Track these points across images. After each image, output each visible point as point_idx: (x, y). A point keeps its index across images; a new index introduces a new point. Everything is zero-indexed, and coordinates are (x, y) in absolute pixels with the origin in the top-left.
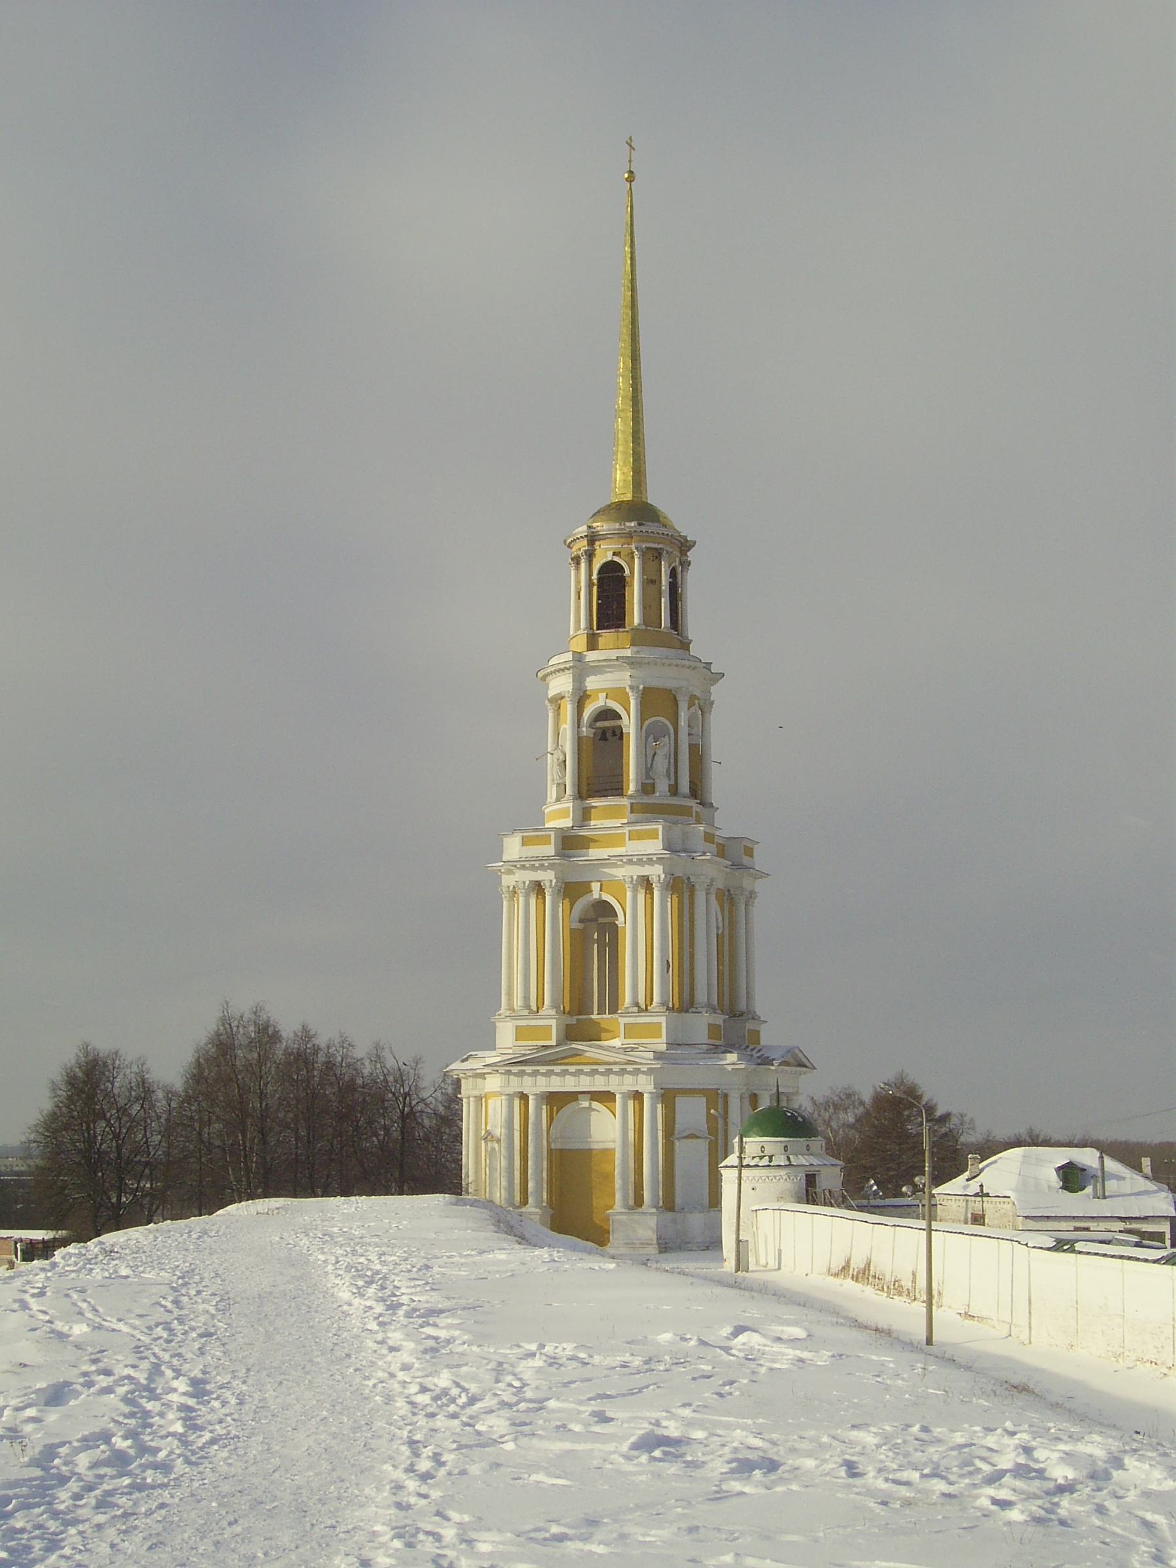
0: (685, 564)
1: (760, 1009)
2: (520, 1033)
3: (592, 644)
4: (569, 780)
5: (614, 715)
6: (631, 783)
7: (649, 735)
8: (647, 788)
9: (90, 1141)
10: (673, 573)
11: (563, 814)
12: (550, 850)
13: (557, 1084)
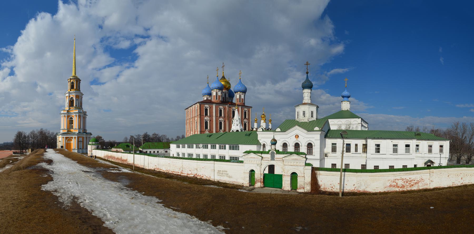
0: (80, 82)
1: (87, 129)
2: (63, 131)
3: (70, 91)
4: (68, 105)
5: (73, 98)
6: (75, 105)
7: (76, 100)
8: (76, 106)
9: (20, 141)
10: (79, 83)
12: (66, 112)
13: (67, 136)
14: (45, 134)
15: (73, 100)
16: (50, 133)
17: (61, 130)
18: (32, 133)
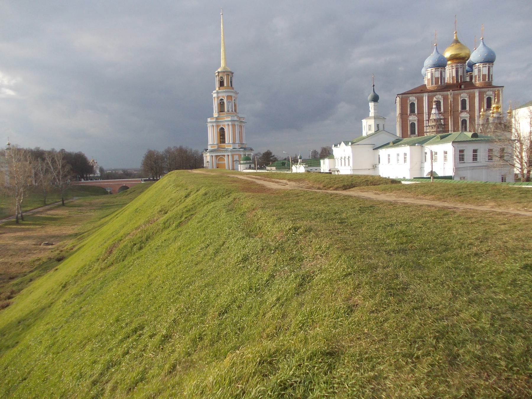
0: (233, 76)
2: (211, 147)
3: (219, 89)
5: (223, 100)
7: (228, 102)
8: (228, 111)
10: (231, 78)
11: (216, 115)
13: (217, 154)
14: (186, 152)
15: (224, 102)
16: (193, 151)
17: (208, 146)
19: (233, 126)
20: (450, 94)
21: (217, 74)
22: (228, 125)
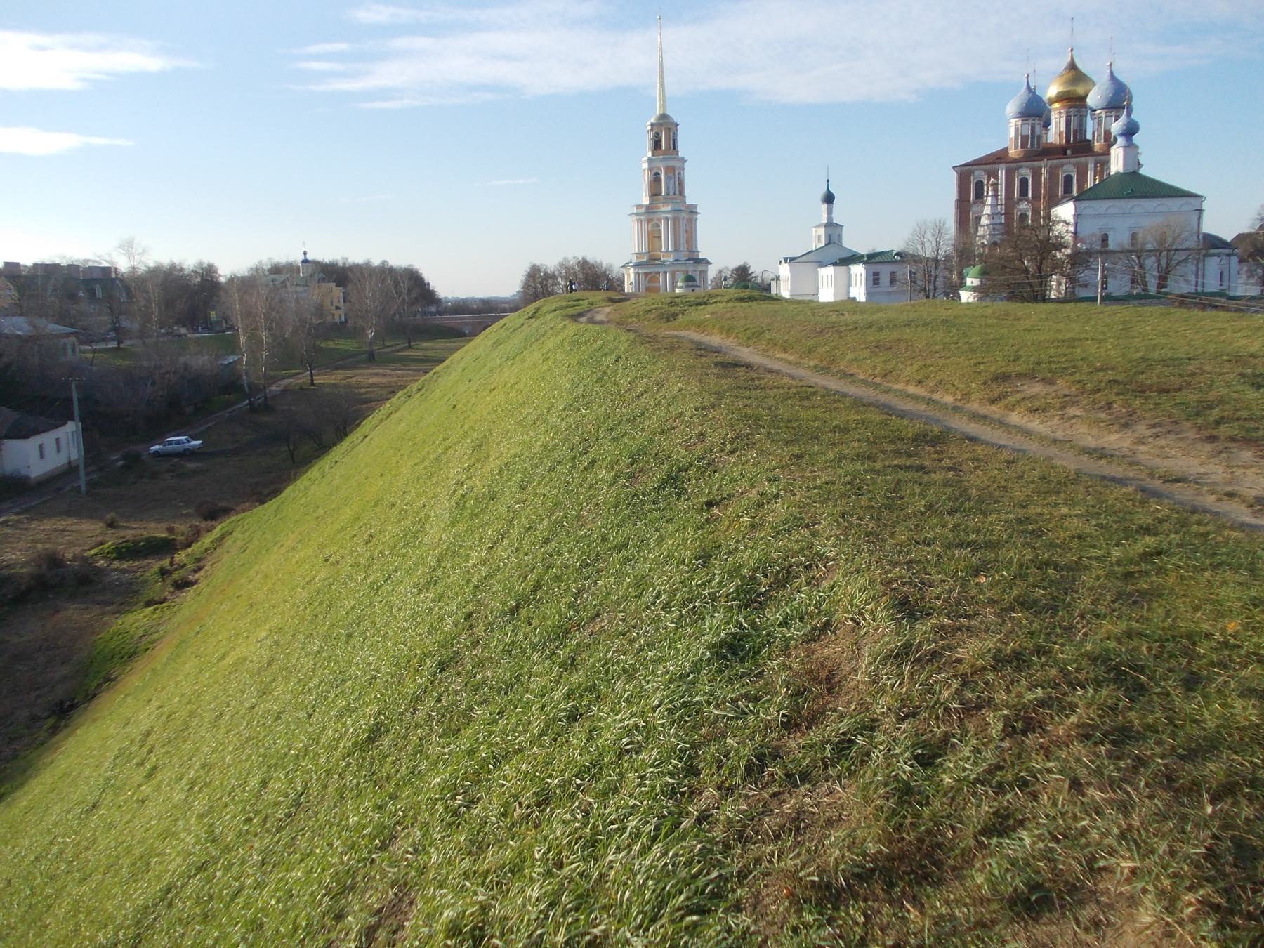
7: (668, 179)
18: (561, 265)
19: (675, 220)
20: (1044, 166)
21: (649, 128)
22: (667, 219)
